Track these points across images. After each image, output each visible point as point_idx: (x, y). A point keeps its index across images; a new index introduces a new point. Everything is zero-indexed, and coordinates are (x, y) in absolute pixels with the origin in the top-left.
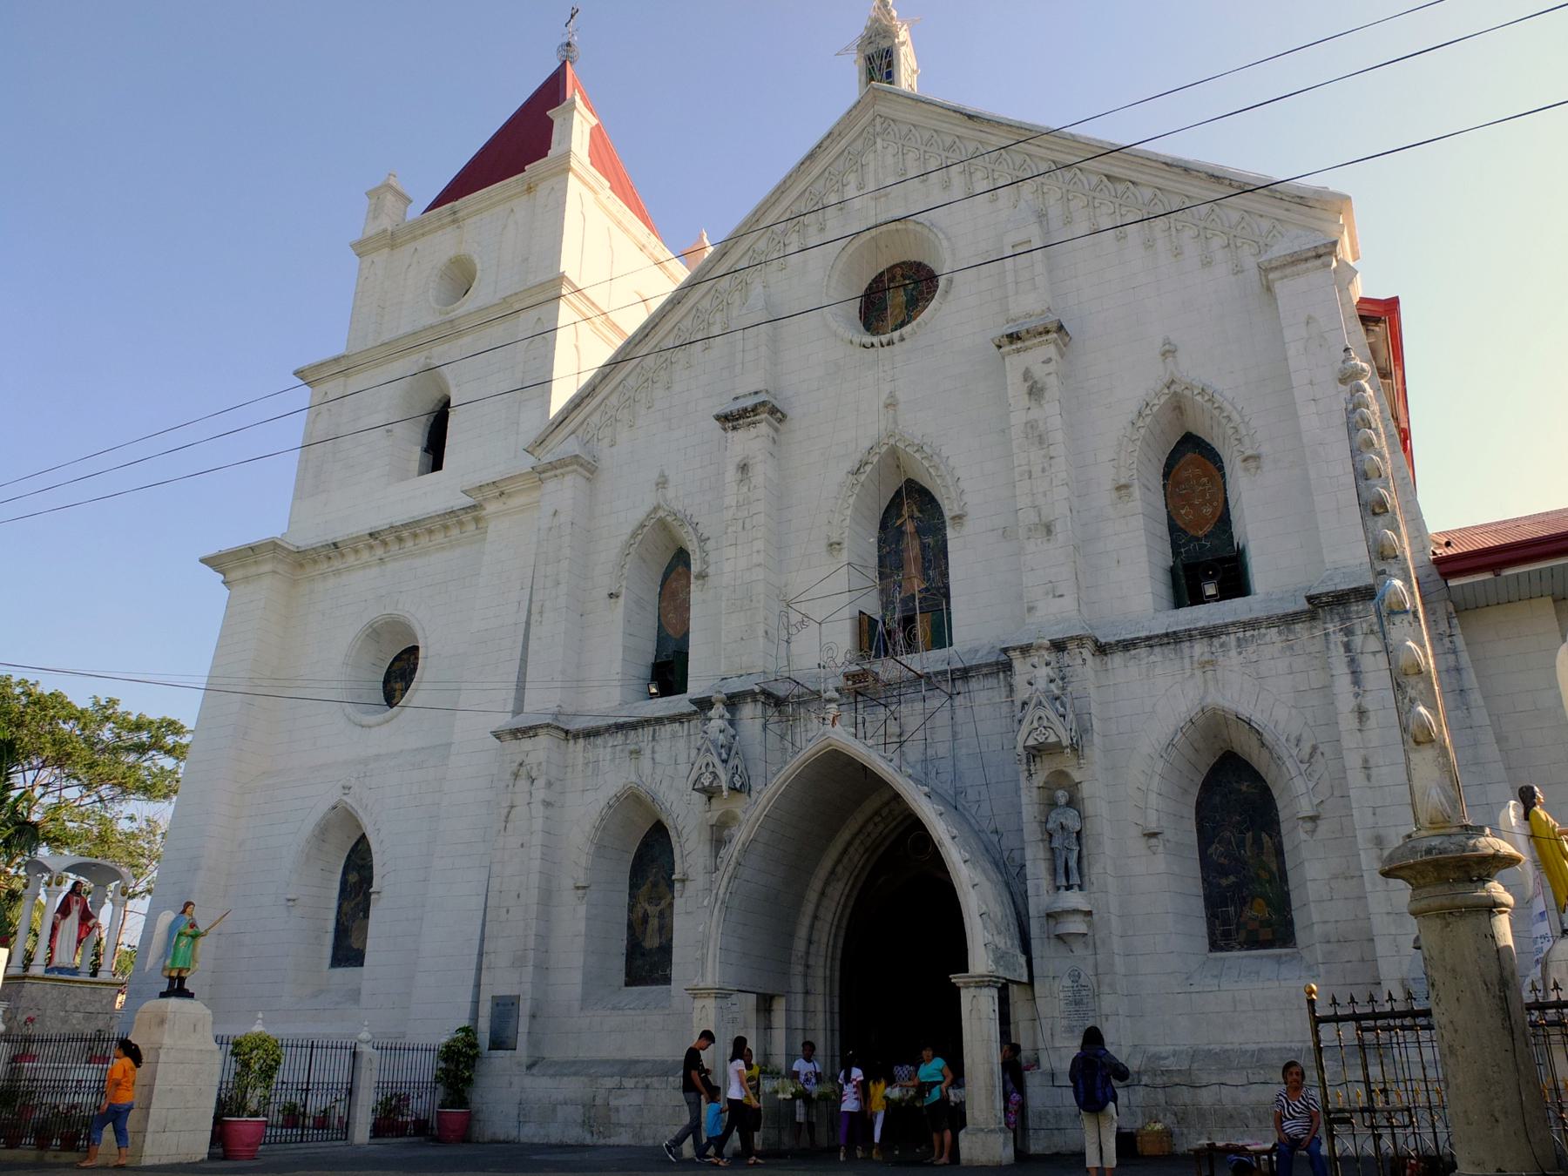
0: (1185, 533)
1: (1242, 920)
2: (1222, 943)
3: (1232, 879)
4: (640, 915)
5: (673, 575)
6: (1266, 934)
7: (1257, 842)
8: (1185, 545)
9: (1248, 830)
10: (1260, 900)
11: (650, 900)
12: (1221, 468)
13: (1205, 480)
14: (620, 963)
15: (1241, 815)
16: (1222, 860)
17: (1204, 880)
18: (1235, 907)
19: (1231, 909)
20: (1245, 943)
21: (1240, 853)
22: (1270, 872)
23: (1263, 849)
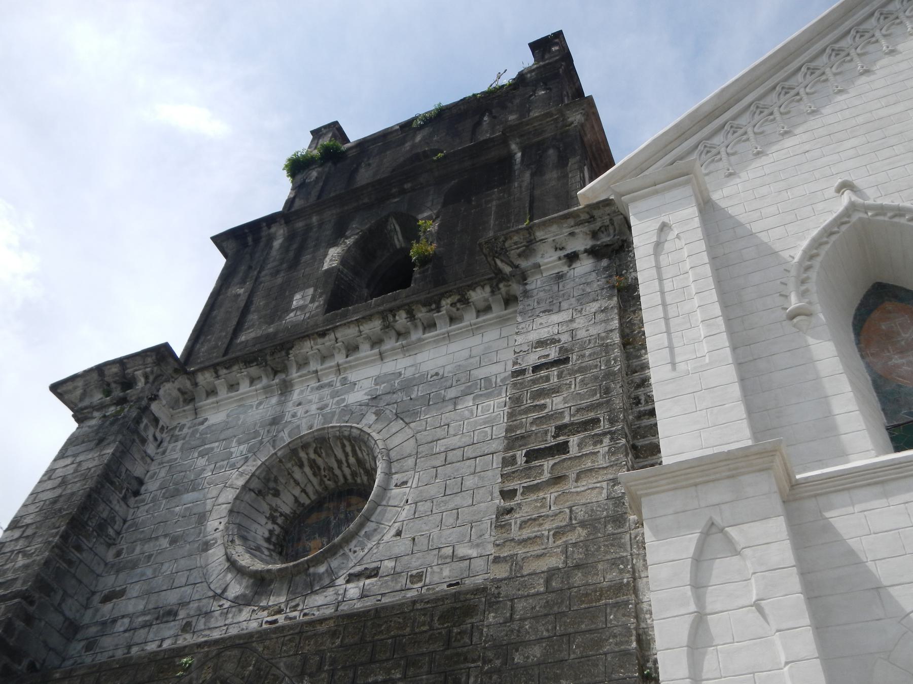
5: (876, 315)
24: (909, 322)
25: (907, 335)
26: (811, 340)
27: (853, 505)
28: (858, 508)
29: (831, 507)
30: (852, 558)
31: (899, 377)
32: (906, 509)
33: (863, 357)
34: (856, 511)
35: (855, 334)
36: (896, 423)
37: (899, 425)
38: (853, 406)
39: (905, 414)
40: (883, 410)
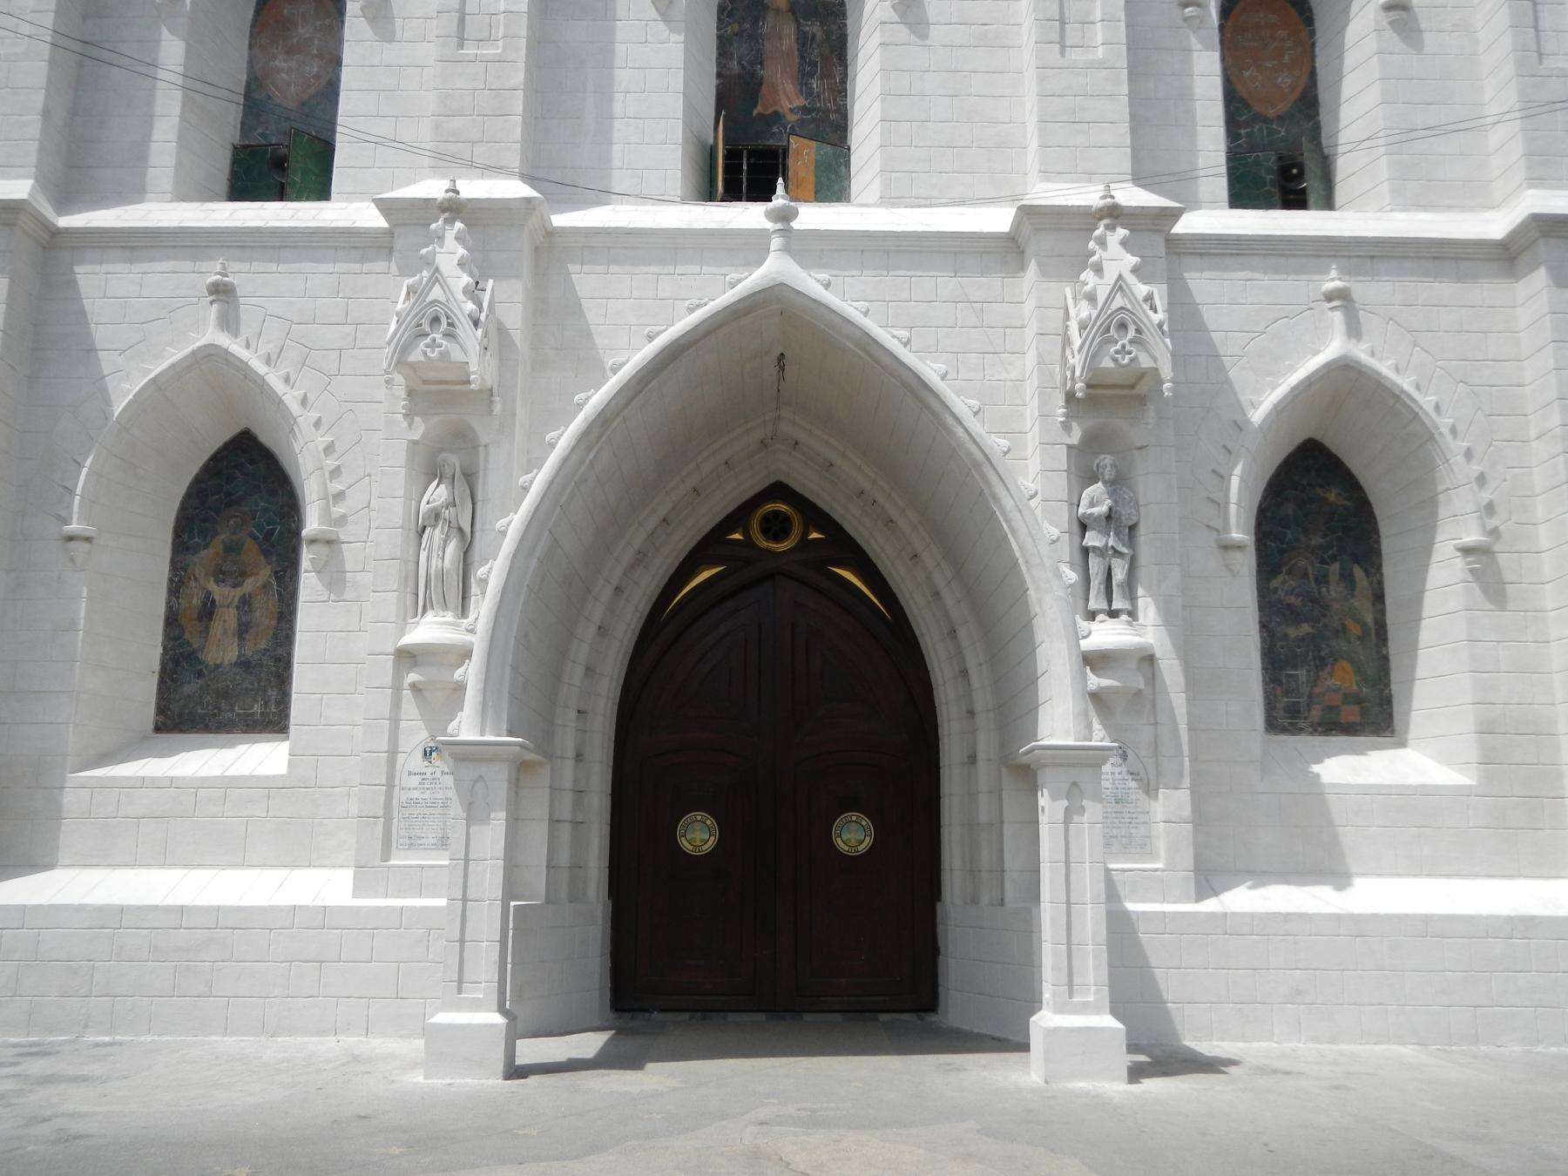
0: (1247, 105)
1: (1317, 690)
2: (1286, 722)
3: (1305, 628)
4: (196, 601)
6: (1351, 714)
7: (1347, 579)
8: (1247, 124)
9: (1334, 559)
10: (1346, 664)
11: (220, 576)
12: (1309, 21)
13: (1282, 33)
14: (146, 691)
15: (1324, 536)
16: (1292, 600)
17: (1264, 626)
18: (1309, 671)
19: (1302, 673)
20: (1320, 725)
21: (1320, 593)
22: (1363, 624)
23: (1353, 589)
24: (312, 13)
25: (303, 31)
26: (165, 34)
27: (101, 263)
28: (106, 267)
29: (81, 262)
30: (81, 317)
31: (273, 85)
32: (142, 279)
33: (250, 47)
34: (102, 271)
35: (255, 11)
36: (247, 143)
37: (248, 146)
38: (173, 136)
39: (260, 135)
40: (242, 124)
